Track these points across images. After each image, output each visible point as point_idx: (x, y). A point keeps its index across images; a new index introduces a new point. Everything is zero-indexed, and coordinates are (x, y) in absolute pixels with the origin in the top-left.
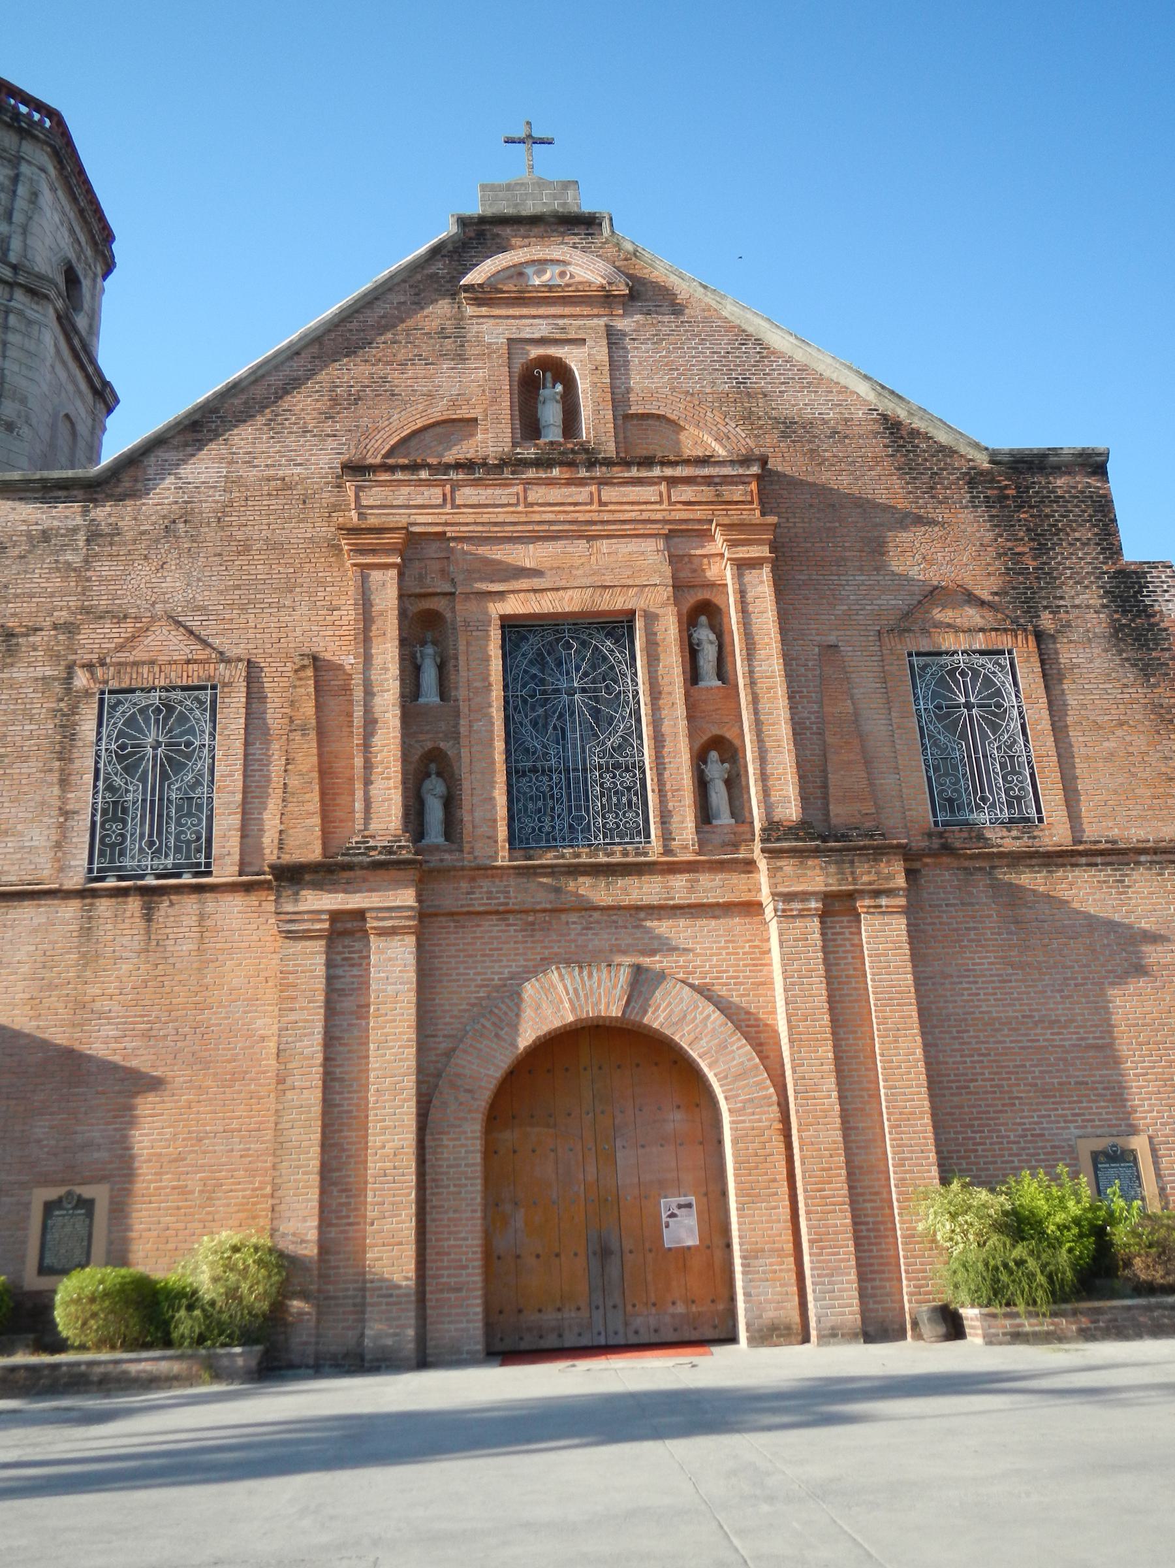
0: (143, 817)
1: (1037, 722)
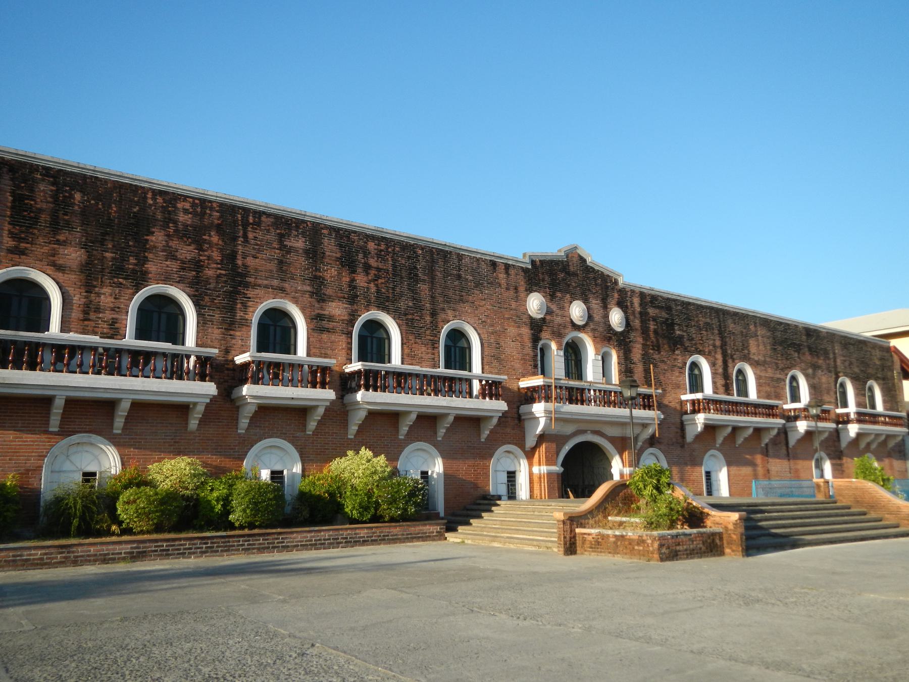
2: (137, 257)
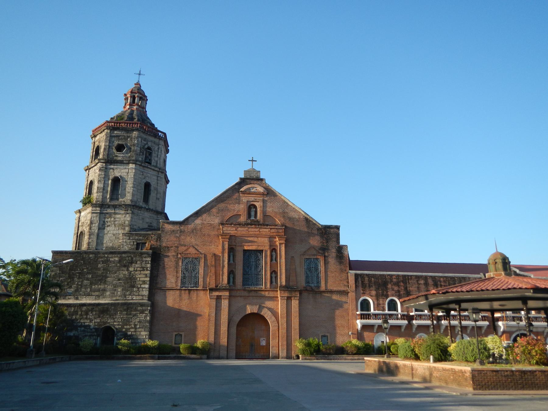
0: (189, 278)
1: (323, 270)
2: (386, 291)
